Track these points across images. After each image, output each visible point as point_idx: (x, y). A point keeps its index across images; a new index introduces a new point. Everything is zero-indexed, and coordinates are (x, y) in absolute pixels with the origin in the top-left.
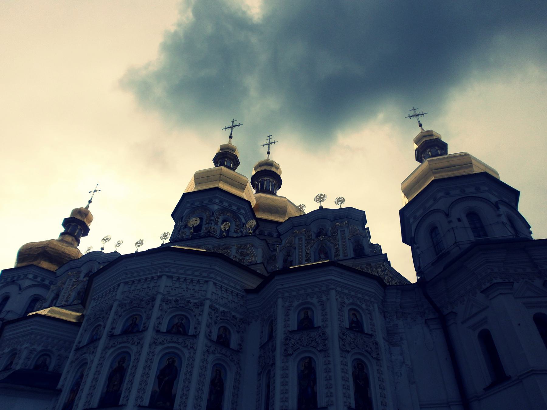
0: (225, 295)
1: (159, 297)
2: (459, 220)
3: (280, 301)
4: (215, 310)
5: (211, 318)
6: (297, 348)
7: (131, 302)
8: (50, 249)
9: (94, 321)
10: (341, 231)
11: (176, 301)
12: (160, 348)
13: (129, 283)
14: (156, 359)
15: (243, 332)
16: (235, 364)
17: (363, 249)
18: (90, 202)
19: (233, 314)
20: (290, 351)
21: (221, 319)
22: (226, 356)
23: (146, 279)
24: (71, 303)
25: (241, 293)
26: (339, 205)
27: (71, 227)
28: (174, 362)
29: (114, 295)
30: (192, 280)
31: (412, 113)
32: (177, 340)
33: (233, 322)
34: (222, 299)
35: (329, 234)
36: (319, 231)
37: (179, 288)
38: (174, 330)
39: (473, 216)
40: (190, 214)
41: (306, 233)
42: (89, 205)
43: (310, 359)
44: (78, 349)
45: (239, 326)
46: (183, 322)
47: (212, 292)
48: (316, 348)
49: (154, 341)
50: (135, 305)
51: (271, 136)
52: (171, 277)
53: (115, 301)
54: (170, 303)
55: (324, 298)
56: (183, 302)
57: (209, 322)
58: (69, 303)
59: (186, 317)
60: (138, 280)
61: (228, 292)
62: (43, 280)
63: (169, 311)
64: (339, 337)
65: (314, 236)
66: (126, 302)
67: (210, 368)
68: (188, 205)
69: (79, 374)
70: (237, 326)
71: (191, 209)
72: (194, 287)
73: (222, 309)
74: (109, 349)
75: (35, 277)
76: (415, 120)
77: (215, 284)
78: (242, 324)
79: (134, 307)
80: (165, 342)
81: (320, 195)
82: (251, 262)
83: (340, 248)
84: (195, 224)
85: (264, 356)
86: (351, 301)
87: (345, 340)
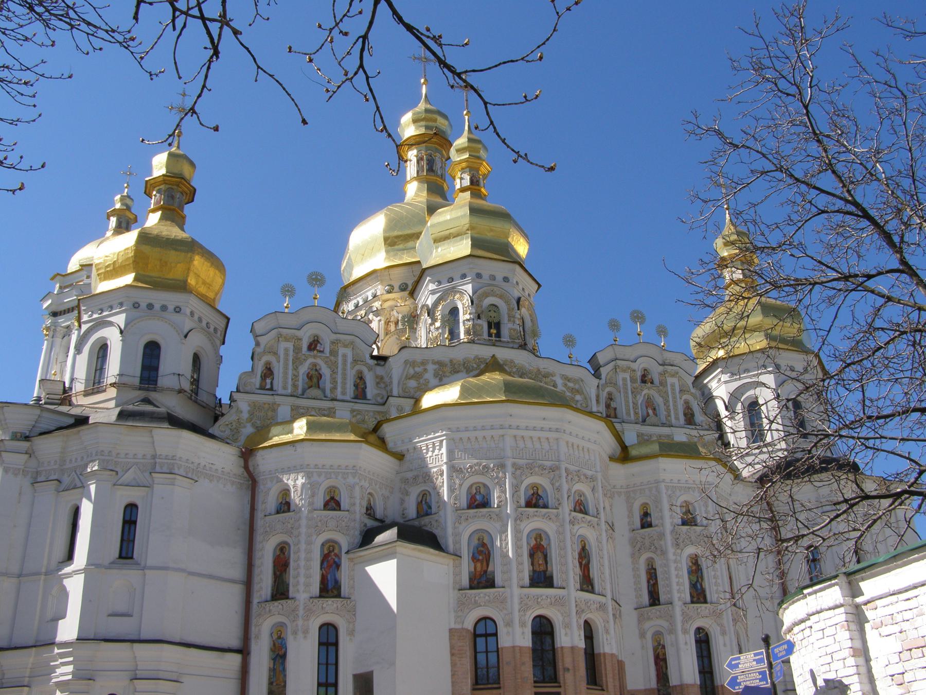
3: (663, 485)
17: (693, 415)
20: (681, 545)
28: (585, 544)
35: (656, 381)
36: (643, 373)
46: (582, 499)
58: (300, 391)
59: (584, 494)
62: (200, 320)
65: (639, 380)
75: (192, 314)
83: (671, 407)
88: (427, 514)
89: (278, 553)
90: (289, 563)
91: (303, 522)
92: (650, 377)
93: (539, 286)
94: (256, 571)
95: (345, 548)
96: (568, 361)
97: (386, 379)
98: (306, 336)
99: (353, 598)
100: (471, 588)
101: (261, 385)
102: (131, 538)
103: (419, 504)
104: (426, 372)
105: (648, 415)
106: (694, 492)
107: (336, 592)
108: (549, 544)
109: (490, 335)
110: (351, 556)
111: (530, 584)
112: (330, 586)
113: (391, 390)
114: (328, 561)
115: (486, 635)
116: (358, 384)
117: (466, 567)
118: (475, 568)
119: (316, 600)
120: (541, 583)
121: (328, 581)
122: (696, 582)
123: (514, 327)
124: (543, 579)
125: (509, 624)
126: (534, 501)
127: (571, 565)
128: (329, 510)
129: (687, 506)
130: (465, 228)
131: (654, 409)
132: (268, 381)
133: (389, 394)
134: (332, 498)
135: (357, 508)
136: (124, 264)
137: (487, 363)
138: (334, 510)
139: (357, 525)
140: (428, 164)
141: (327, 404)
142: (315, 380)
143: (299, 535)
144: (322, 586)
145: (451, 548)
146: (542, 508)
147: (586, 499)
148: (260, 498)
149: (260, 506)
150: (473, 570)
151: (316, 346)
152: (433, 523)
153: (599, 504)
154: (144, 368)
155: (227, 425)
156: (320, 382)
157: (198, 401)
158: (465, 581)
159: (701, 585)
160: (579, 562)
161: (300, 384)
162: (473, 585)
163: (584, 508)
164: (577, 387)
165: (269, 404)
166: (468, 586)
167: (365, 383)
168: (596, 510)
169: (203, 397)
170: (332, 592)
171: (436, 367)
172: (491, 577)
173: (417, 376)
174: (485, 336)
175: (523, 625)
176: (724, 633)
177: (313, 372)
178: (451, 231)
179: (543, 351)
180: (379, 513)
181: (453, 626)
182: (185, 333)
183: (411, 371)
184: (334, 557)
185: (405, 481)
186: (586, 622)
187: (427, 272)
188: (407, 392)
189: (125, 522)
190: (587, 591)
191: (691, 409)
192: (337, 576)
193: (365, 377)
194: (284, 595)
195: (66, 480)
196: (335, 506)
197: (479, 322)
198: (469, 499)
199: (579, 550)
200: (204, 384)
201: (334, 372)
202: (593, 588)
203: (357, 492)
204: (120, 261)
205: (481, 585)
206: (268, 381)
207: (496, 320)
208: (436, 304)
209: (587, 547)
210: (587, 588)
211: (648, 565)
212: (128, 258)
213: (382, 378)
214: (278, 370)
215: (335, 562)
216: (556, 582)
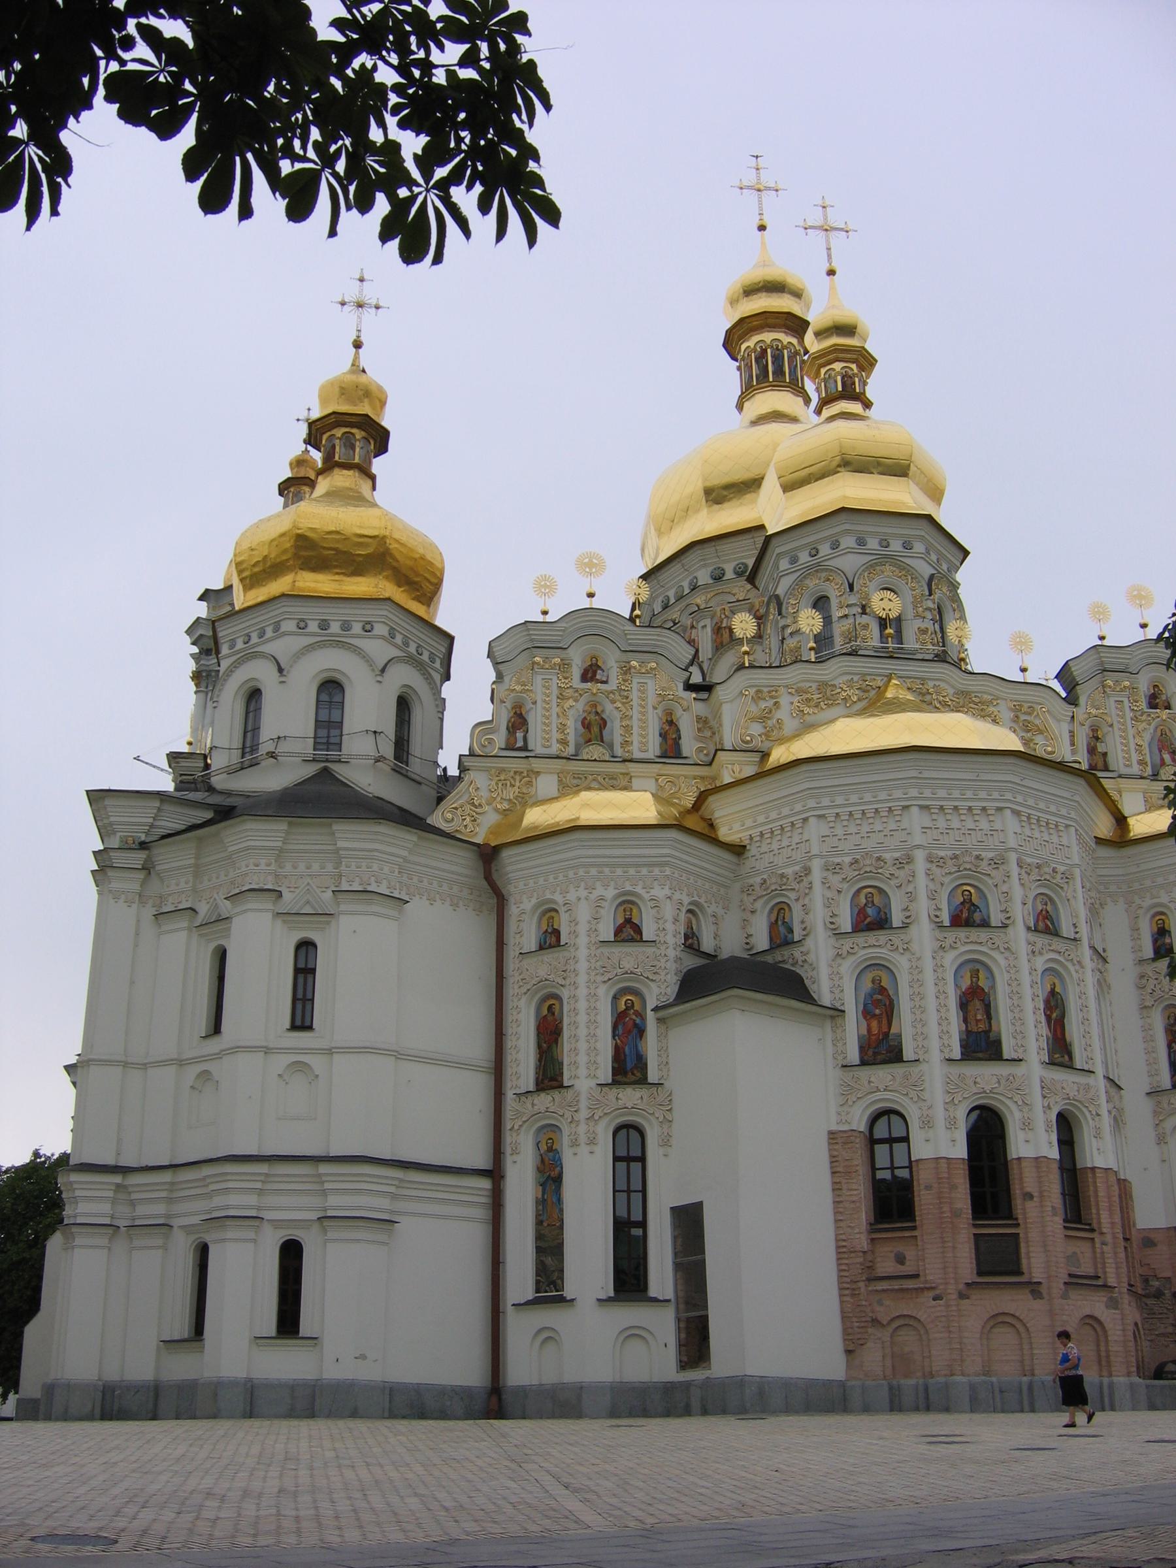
8: (396, 546)
11: (1039, 867)
18: (358, 345)
27: (358, 443)
29: (892, 826)
38: (1040, 923)
40: (866, 574)
42: (357, 354)
46: (1049, 908)
51: (754, 156)
58: (571, 750)
59: (1051, 899)
62: (406, 644)
66: (942, 853)
69: (867, 985)
75: (392, 634)
82: (1052, 753)
88: (788, 942)
89: (545, 1012)
90: (562, 1029)
91: (583, 966)
93: (966, 553)
94: (509, 1042)
95: (651, 1003)
96: (1019, 677)
97: (713, 723)
98: (577, 659)
99: (667, 1084)
100: (864, 1063)
101: (508, 740)
102: (309, 996)
103: (773, 926)
104: (777, 708)
107: (638, 1074)
108: (993, 987)
109: (883, 638)
110: (661, 1014)
111: (962, 1054)
112: (629, 1065)
113: (721, 739)
114: (624, 1024)
115: (891, 1141)
116: (666, 733)
117: (853, 1028)
118: (869, 1030)
119: (605, 1089)
120: (981, 1052)
121: (625, 1055)
123: (923, 626)
124: (983, 1044)
125: (927, 1123)
126: (965, 915)
127: (1030, 1019)
128: (624, 941)
130: (835, 463)
132: (519, 735)
133: (719, 747)
134: (628, 921)
135: (671, 940)
136: (278, 560)
137: (879, 688)
138: (632, 940)
139: (672, 966)
140: (773, 363)
141: (619, 768)
142: (595, 729)
143: (575, 985)
144: (616, 1065)
145: (826, 1001)
146: (979, 926)
147: (1056, 909)
148: (511, 926)
149: (511, 938)
150: (866, 1033)
151: (595, 673)
152: (797, 954)
153: (1077, 916)
154: (318, 723)
155: (456, 808)
156: (605, 732)
157: (409, 774)
158: (854, 1055)
160: (1045, 1014)
161: (571, 739)
162: (866, 1058)
163: (1053, 924)
164: (1037, 722)
165: (522, 773)
166: (857, 1062)
167: (678, 730)
168: (1072, 929)
169: (416, 767)
170: (633, 1074)
171: (796, 699)
172: (896, 1044)
173: (763, 718)
174: (875, 642)
175: (951, 1124)
177: (593, 717)
178: (812, 469)
179: (976, 664)
180: (707, 945)
181: (834, 1128)
182: (380, 667)
183: (754, 709)
184: (634, 1017)
185: (748, 890)
186: (1060, 1116)
187: (774, 542)
188: (747, 742)
189: (297, 971)
192: (639, 1045)
193: (678, 720)
194: (556, 1080)
195: (203, 909)
196: (632, 933)
197: (865, 619)
198: (855, 915)
199: (1046, 994)
200: (417, 747)
201: (625, 717)
203: (669, 911)
204: (272, 556)
205: (879, 1057)
206: (519, 735)
207: (893, 615)
208: (791, 591)
209: (1057, 989)
210: (1060, 1060)
212: (285, 551)
213: (706, 721)
214: (535, 720)
215: (635, 1025)
216: (1007, 1052)
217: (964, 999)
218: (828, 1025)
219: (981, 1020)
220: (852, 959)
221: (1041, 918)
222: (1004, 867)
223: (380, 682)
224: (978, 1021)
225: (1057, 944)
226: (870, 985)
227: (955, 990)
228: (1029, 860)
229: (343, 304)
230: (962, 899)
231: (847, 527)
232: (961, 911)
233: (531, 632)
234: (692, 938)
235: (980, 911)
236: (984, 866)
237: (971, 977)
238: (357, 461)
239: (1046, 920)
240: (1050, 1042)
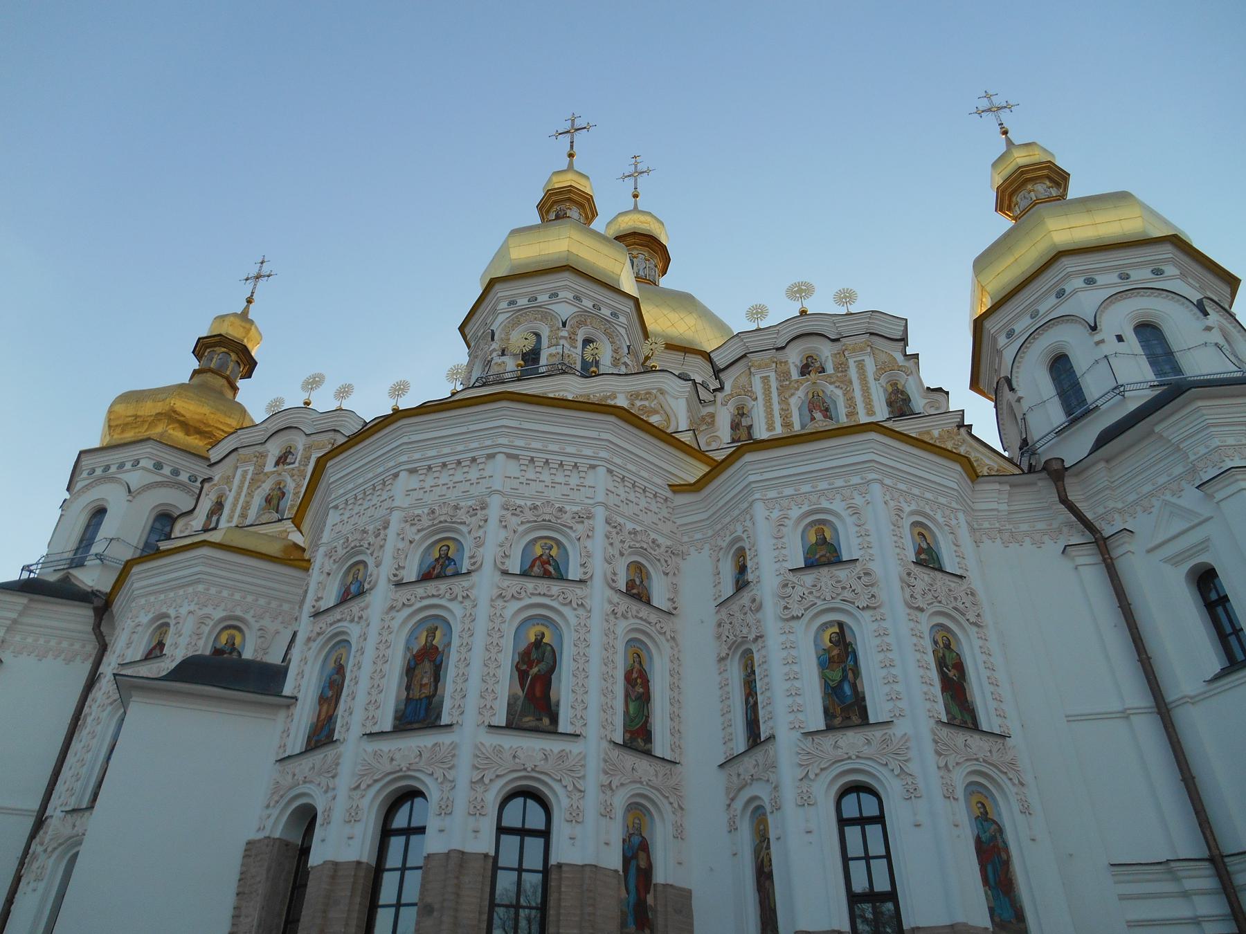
0: (632, 497)
1: (495, 502)
2: (1120, 339)
4: (619, 528)
5: (611, 544)
6: (812, 603)
7: (433, 512)
9: (347, 552)
10: (855, 362)
11: (535, 508)
12: (516, 606)
13: (420, 472)
14: (509, 631)
15: (674, 574)
16: (668, 641)
17: (907, 400)
19: (653, 536)
21: (630, 547)
22: (650, 623)
23: (459, 462)
24: (255, 521)
25: (664, 493)
26: (843, 306)
28: (543, 634)
30: (561, 465)
31: (984, 104)
32: (548, 591)
33: (653, 552)
34: (627, 504)
35: (830, 369)
37: (536, 481)
38: (536, 569)
39: (1148, 331)
41: (776, 367)
42: (247, 307)
43: (841, 625)
44: (316, 615)
45: (666, 561)
46: (554, 553)
47: (607, 490)
48: (854, 603)
49: (501, 592)
50: (442, 519)
52: (516, 457)
53: (391, 509)
54: (521, 512)
55: (858, 500)
56: (548, 510)
57: (610, 553)
59: (559, 543)
60: (440, 464)
61: (637, 489)
62: (176, 472)
63: (521, 529)
64: (902, 580)
65: (795, 375)
67: (620, 646)
68: (503, 305)
69: (331, 665)
70: (663, 561)
71: (508, 315)
72: (567, 478)
73: (630, 526)
74: (398, 611)
75: (159, 466)
76: (990, 120)
77: (610, 471)
78: (671, 557)
79: (441, 522)
80: (523, 594)
81: (799, 285)
84: (524, 346)
85: (731, 623)
86: (913, 507)
87: (913, 586)
92: (817, 365)
101: (203, 527)
105: (813, 419)
106: (830, 500)
108: (449, 644)
122: (841, 681)
129: (820, 532)
131: (827, 410)
150: (315, 720)
151: (286, 457)
156: (282, 503)
159: (854, 687)
163: (557, 568)
176: (912, 794)
190: (536, 730)
191: (903, 392)
197: (503, 358)
199: (523, 647)
202: (554, 719)
203: (188, 626)
206: (214, 518)
210: (533, 724)
211: (747, 666)
217: (412, 663)
218: (282, 715)
219: (426, 684)
220: (321, 637)
221: (538, 563)
222: (484, 512)
223: (131, 501)
224: (421, 686)
225: (555, 588)
226: (333, 665)
227: (406, 654)
228: (522, 503)
229: (247, 279)
230: (437, 556)
231: (499, 295)
232: (434, 568)
233: (241, 437)
234: (230, 653)
235: (455, 564)
236: (462, 515)
237: (427, 637)
238: (212, 366)
239: (548, 567)
240: (520, 703)
